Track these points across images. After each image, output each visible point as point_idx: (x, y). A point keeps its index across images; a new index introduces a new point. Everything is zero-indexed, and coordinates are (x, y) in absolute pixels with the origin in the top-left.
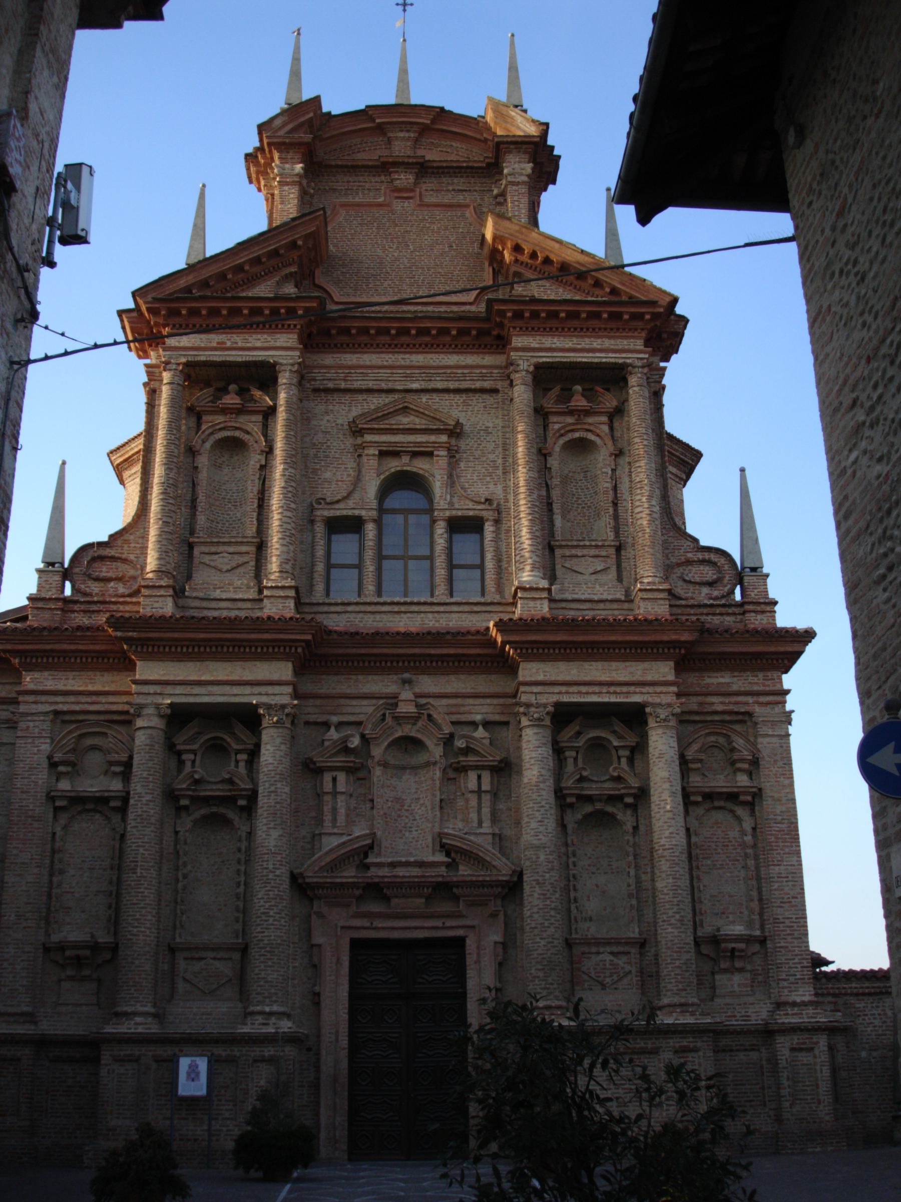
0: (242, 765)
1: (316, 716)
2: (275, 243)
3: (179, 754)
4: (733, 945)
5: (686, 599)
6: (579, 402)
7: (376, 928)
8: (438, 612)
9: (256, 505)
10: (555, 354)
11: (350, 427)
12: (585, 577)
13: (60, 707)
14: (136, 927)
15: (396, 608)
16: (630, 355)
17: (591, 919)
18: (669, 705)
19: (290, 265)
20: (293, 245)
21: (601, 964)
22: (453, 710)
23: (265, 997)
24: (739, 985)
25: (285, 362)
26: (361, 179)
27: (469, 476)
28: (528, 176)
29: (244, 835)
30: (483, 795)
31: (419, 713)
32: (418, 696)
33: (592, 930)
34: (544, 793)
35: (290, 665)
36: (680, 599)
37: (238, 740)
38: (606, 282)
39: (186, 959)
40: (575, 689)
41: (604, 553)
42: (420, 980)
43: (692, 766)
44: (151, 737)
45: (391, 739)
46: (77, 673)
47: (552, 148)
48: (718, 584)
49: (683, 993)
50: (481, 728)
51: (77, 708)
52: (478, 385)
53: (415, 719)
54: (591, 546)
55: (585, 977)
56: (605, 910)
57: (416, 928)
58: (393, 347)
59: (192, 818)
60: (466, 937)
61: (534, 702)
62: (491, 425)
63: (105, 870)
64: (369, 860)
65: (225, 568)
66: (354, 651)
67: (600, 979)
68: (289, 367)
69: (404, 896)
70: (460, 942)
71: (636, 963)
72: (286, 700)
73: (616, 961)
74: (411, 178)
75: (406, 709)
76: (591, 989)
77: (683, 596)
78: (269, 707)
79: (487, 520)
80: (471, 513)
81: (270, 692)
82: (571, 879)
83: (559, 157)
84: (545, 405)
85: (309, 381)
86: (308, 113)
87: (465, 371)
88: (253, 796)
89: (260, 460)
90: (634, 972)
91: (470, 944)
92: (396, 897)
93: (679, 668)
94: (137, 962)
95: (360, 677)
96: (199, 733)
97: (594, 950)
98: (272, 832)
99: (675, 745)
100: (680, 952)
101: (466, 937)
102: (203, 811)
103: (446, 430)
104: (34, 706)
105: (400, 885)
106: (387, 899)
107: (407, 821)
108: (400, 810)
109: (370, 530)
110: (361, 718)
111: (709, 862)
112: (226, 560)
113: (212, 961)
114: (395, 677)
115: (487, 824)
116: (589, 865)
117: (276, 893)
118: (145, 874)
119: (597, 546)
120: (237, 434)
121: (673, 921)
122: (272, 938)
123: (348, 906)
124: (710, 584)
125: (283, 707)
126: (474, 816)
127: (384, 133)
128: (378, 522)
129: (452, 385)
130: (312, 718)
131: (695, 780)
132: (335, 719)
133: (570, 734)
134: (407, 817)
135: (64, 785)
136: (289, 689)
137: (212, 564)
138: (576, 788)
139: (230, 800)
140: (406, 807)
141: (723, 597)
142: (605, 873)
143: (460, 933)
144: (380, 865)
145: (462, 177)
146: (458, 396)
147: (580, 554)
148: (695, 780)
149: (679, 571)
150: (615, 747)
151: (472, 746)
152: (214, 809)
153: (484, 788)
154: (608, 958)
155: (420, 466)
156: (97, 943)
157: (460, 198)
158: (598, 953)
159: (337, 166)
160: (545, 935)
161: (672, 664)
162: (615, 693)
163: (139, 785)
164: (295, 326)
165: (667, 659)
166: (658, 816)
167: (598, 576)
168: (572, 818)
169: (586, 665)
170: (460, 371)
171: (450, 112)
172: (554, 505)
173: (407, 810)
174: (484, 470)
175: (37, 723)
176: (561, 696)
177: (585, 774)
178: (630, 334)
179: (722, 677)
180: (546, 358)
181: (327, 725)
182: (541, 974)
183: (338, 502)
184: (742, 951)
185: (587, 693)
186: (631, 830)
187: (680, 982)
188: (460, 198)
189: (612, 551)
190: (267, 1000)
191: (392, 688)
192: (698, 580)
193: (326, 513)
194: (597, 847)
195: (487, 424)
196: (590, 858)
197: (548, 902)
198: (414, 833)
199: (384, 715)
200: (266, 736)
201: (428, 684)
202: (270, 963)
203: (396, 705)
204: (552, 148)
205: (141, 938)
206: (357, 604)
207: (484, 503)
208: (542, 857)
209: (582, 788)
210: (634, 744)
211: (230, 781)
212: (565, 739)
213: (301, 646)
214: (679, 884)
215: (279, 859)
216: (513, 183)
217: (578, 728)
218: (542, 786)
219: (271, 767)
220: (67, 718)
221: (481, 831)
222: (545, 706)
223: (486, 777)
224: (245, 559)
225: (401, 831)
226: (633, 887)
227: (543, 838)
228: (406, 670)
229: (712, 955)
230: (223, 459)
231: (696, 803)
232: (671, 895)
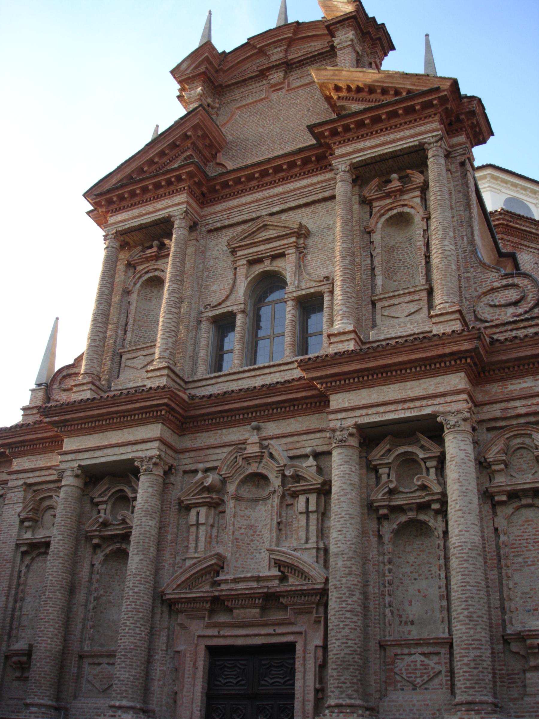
1: (190, 466)
2: (172, 138)
5: (492, 321)
7: (224, 637)
10: (365, 153)
12: (400, 320)
13: (29, 481)
14: (40, 637)
15: (253, 373)
16: (426, 136)
17: (412, 623)
19: (186, 150)
20: (186, 137)
21: (412, 664)
22: (291, 446)
23: (117, 694)
25: (176, 214)
26: (250, 87)
27: (313, 264)
30: (311, 515)
31: (262, 452)
34: (344, 505)
36: (486, 322)
38: (402, 88)
39: (90, 664)
40: (373, 410)
41: (416, 297)
42: (263, 682)
43: (494, 467)
45: (242, 476)
46: (43, 455)
48: (523, 302)
49: (471, 691)
51: (40, 480)
52: (320, 196)
54: (405, 294)
56: (427, 613)
57: (255, 635)
59: (103, 554)
60: (296, 642)
66: (213, 409)
67: (411, 679)
69: (242, 608)
70: (290, 647)
71: (446, 663)
72: (156, 452)
73: (426, 661)
74: (281, 75)
75: (253, 449)
76: (402, 690)
77: (489, 318)
78: (142, 460)
79: (324, 292)
80: (312, 290)
81: (144, 449)
82: (387, 585)
84: (367, 195)
86: (204, 54)
87: (310, 189)
90: (443, 672)
94: (38, 664)
95: (224, 431)
96: (108, 488)
97: (406, 651)
100: (468, 649)
101: (296, 642)
103: (293, 233)
104: (16, 482)
105: (237, 597)
106: (230, 610)
107: (258, 544)
108: (253, 535)
111: (520, 560)
112: (141, 361)
113: (106, 666)
114: (248, 427)
115: (313, 539)
116: (411, 572)
117: (133, 606)
118: (51, 596)
119: (410, 293)
121: (461, 618)
122: (127, 644)
124: (515, 304)
125: (151, 458)
127: (265, 54)
129: (301, 202)
130: (188, 468)
131: (500, 480)
132: (201, 466)
133: (381, 453)
134: (258, 541)
135: (28, 535)
137: (132, 365)
140: (258, 533)
141: (526, 312)
142: (427, 578)
143: (290, 639)
144: (226, 581)
145: (317, 63)
146: (308, 209)
147: (396, 302)
149: (485, 300)
150: (423, 459)
151: (300, 474)
152: (118, 545)
154: (419, 658)
155: (278, 265)
158: (410, 654)
159: (233, 84)
160: (339, 637)
162: (409, 408)
164: (184, 188)
165: (456, 372)
167: (412, 317)
168: (388, 529)
169: (385, 388)
170: (306, 190)
171: (304, 23)
173: (259, 535)
174: (325, 257)
175: (16, 494)
176: (362, 418)
178: (426, 121)
179: (524, 382)
180: (357, 158)
181: (196, 471)
183: (220, 304)
185: (385, 412)
187: (468, 680)
190: (119, 696)
192: (502, 302)
193: (210, 314)
194: (419, 555)
195: (329, 223)
196: (412, 565)
197: (344, 605)
198: (263, 554)
199: (236, 457)
202: (123, 665)
205: (43, 645)
207: (323, 281)
208: (340, 563)
210: (439, 454)
212: (377, 457)
213: (163, 409)
214: (468, 580)
215: (138, 578)
217: (388, 447)
218: (342, 499)
220: (36, 488)
221: (307, 546)
222: (347, 428)
225: (252, 553)
227: (342, 546)
228: (255, 419)
229: (522, 652)
230: (153, 294)
231: (502, 503)
232: (460, 592)
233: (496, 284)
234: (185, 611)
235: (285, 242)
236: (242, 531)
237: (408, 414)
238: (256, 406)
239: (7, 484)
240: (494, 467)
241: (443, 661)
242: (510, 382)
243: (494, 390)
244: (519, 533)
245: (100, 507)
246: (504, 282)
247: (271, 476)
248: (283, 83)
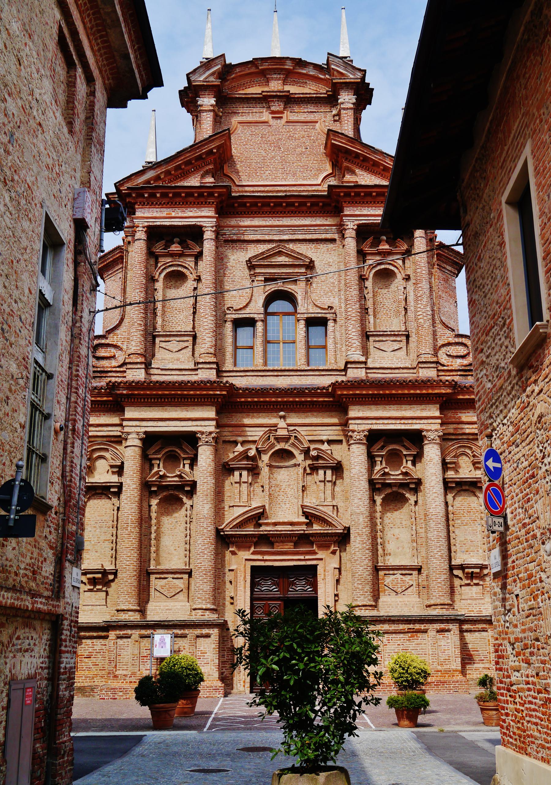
0: (187, 466)
3: (151, 460)
4: (472, 570)
5: (448, 366)
6: (385, 247)
8: (301, 375)
9: (192, 312)
10: (370, 218)
11: (247, 264)
15: (276, 374)
18: (436, 430)
19: (209, 164)
22: (310, 433)
24: (476, 593)
25: (207, 225)
28: (353, 104)
29: (189, 507)
32: (289, 425)
33: (392, 561)
34: (362, 482)
35: (214, 408)
37: (185, 452)
40: (381, 421)
43: (449, 466)
44: (135, 451)
45: (273, 450)
47: (369, 84)
49: (442, 598)
50: (326, 443)
52: (323, 236)
53: (286, 439)
55: (386, 588)
61: (356, 429)
62: (331, 261)
63: (109, 527)
64: (261, 521)
65: (175, 350)
68: (210, 229)
72: (212, 429)
75: (282, 433)
77: (446, 364)
78: (202, 433)
80: (320, 315)
83: (373, 89)
85: (222, 235)
86: (217, 65)
88: (194, 484)
89: (193, 284)
91: (320, 570)
92: (277, 542)
93: (442, 410)
98: (205, 505)
99: (440, 454)
102: (165, 494)
109: (260, 326)
110: (256, 438)
114: (275, 414)
115: (330, 499)
119: (395, 335)
120: (180, 269)
123: (249, 548)
124: (463, 357)
125: (211, 433)
126: (322, 495)
128: (264, 321)
130: (227, 438)
132: (240, 439)
136: (214, 423)
137: (167, 348)
138: (381, 479)
139: (180, 488)
144: (267, 524)
148: (451, 474)
149: (444, 350)
153: (327, 479)
155: (290, 287)
156: (105, 570)
157: (311, 117)
158: (394, 574)
161: (438, 406)
163: (128, 479)
164: (213, 203)
166: (429, 495)
171: (305, 62)
172: (369, 310)
177: (386, 470)
180: (363, 221)
181: (236, 443)
182: (360, 587)
184: (477, 573)
186: (413, 503)
188: (311, 117)
189: (404, 338)
191: (274, 421)
192: (455, 354)
195: (329, 260)
197: (365, 545)
199: (269, 436)
200: (200, 450)
201: (294, 419)
203: (276, 431)
204: (369, 84)
206: (253, 371)
207: (327, 309)
208: (361, 520)
209: (385, 479)
211: (180, 476)
216: (344, 109)
218: (361, 478)
219: (204, 468)
222: (363, 431)
223: (329, 472)
224: (186, 344)
226: (414, 536)
233: (451, 340)
234: (237, 542)
235: (297, 270)
237: (403, 427)
240: (449, 466)
241: (414, 579)
243: (449, 415)
244: (459, 505)
245: (153, 462)
246: (457, 340)
247: (296, 452)
248: (282, 113)
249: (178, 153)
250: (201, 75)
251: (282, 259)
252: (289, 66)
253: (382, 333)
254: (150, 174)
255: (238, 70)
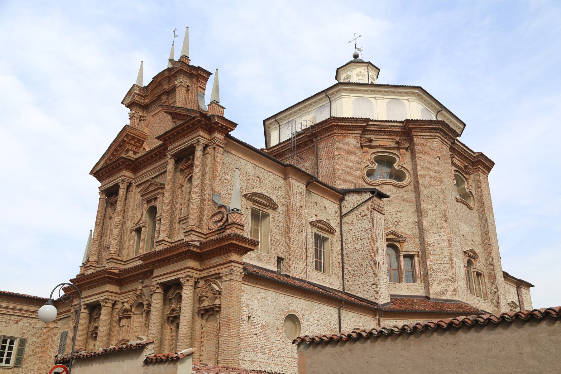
58: (153, 162)
124: (221, 220)
147: (186, 221)
178: (196, 131)
228: (141, 278)
236: (137, 327)
238: (139, 273)
239: (71, 311)
242: (211, 259)
249: (109, 147)
250: (128, 101)
251: (152, 188)
252: (167, 74)
253: (184, 218)
254: (102, 163)
255: (150, 88)
